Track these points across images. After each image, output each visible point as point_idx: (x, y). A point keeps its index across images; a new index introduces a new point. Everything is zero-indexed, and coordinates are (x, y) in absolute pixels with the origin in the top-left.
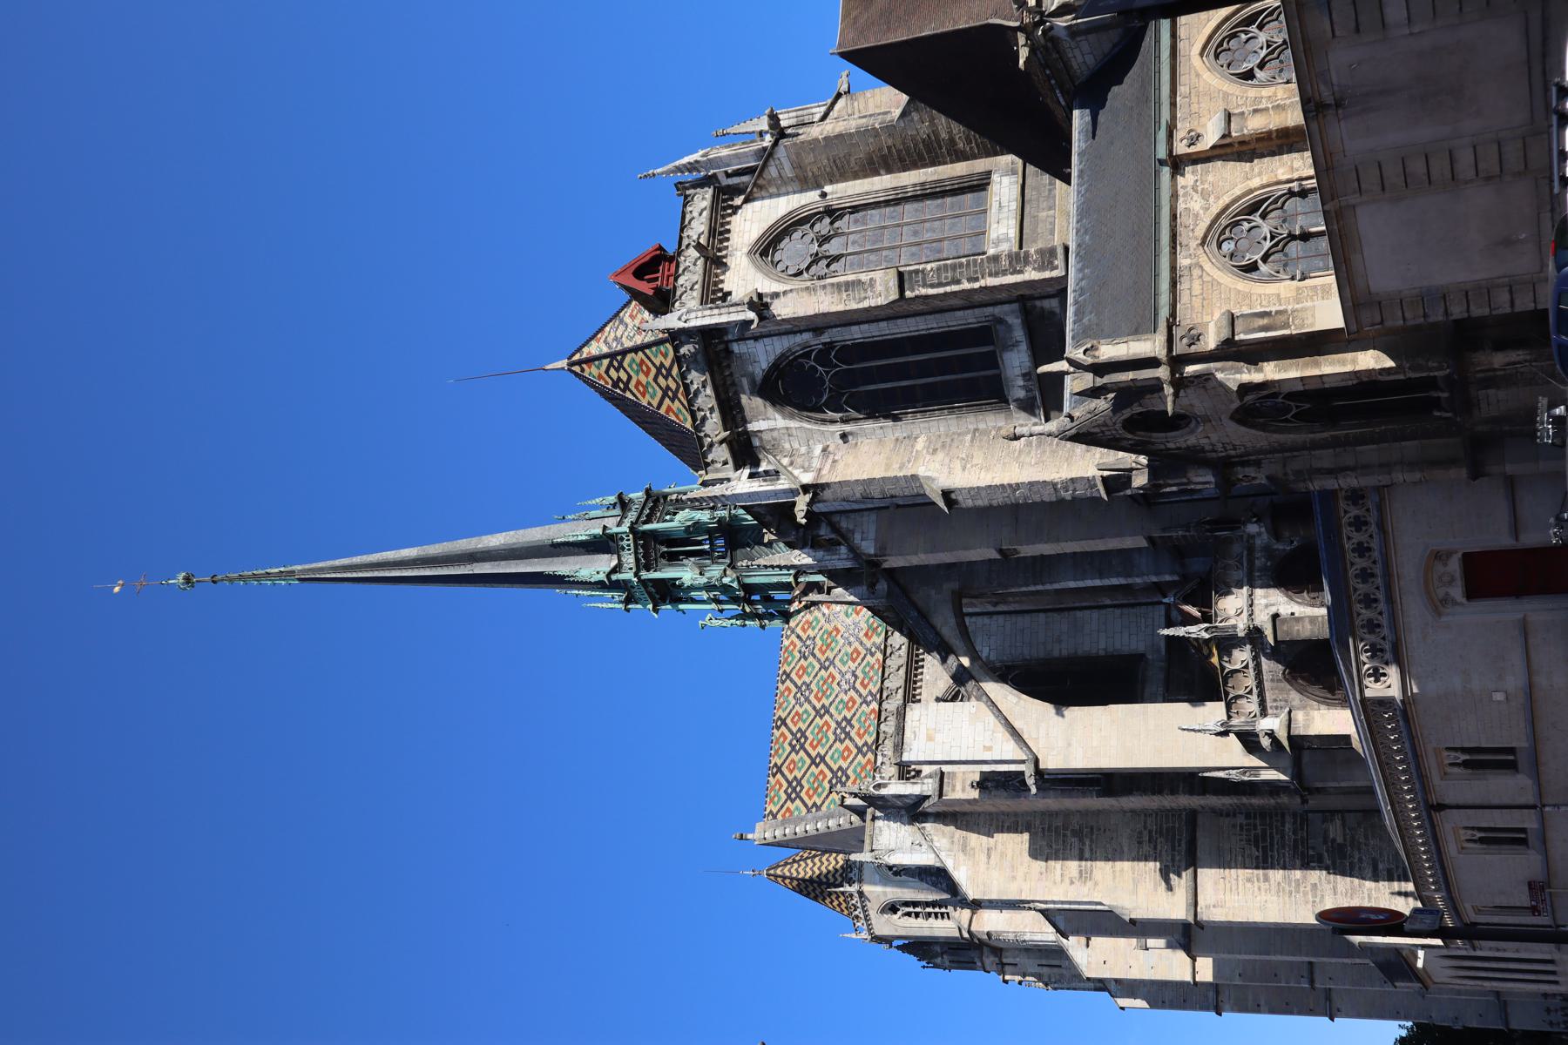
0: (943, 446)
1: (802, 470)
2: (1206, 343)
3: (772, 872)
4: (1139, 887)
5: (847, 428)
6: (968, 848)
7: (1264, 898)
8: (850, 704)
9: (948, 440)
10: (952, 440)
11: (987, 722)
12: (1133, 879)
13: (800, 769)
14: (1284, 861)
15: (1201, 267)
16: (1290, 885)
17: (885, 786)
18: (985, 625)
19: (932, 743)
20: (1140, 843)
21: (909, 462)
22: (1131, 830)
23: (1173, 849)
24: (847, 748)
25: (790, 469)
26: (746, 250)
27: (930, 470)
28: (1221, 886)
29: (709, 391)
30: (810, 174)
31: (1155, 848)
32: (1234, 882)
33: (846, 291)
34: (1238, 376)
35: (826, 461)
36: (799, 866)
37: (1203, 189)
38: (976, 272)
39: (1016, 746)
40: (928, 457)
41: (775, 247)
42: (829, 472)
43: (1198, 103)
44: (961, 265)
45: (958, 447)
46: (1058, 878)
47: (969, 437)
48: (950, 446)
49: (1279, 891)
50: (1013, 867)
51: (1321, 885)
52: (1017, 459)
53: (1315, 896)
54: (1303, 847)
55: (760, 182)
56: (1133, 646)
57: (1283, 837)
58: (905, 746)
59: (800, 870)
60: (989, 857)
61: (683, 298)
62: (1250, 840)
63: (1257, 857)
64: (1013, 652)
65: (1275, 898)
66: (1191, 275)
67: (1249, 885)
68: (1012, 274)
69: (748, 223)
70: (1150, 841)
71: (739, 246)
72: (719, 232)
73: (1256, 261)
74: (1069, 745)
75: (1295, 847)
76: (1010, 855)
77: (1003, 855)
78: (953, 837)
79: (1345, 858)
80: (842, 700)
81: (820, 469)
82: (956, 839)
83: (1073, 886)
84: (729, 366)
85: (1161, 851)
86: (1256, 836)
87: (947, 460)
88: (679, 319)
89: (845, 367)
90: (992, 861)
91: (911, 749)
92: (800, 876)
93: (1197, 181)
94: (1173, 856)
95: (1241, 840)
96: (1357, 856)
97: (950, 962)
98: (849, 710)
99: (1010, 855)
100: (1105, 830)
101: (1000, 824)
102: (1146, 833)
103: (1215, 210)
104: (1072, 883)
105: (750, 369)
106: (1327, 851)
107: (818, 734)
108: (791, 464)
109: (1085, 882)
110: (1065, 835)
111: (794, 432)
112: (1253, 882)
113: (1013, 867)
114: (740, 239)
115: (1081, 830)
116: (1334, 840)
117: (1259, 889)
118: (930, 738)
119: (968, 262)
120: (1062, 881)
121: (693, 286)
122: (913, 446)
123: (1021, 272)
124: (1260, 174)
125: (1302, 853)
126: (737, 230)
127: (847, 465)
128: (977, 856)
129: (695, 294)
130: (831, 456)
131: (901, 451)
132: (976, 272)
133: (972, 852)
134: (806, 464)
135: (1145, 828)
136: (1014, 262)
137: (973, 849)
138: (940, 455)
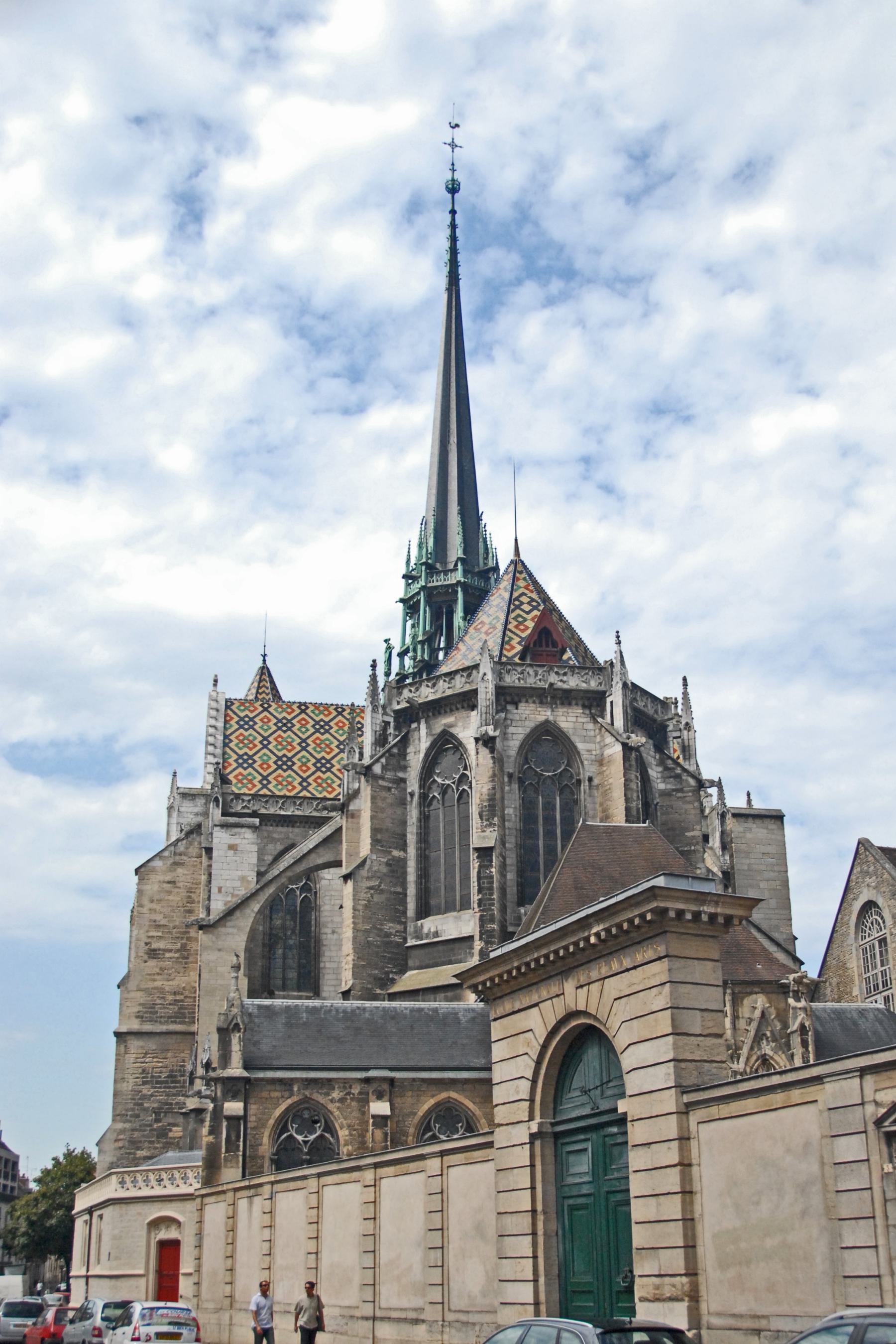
0: (393, 871)
1: (384, 764)
2: (230, 1101)
4: (142, 993)
5: (416, 798)
6: (176, 867)
7: (131, 1081)
8: (304, 768)
9: (399, 874)
10: (398, 878)
12: (148, 988)
13: (261, 727)
14: (157, 1096)
15: (290, 1097)
16: (140, 1099)
17: (218, 806)
20: (175, 993)
21: (382, 846)
22: (184, 987)
23: (169, 1017)
24: (269, 766)
25: (387, 755)
26: (551, 718)
27: (372, 862)
28: (140, 1051)
29: (449, 692)
30: (605, 769)
31: (170, 1004)
32: (143, 1060)
33: (489, 805)
34: (208, 1119)
35: (390, 782)
37: (347, 1099)
38: (485, 905)
40: (385, 860)
41: (553, 741)
42: (380, 786)
43: (412, 1096)
44: (492, 894)
45: (391, 882)
46: (151, 934)
47: (399, 890)
48: (393, 876)
49: (135, 1091)
51: (139, 1121)
52: (374, 927)
53: (131, 1116)
54: (167, 1109)
55: (603, 730)
56: (325, 988)
57: (174, 1095)
60: (169, 882)
61: (514, 672)
62: (173, 1072)
63: (160, 1077)
65: (130, 1089)
66: (285, 1091)
67: (140, 1070)
68: (480, 932)
69: (574, 719)
70: (175, 1000)
71: (555, 713)
72: (566, 698)
73: (289, 1131)
74: (220, 950)
75: (167, 1104)
76: (171, 898)
79: (158, 1137)
80: (309, 761)
81: (382, 778)
83: (143, 944)
84: (463, 707)
85: (168, 1008)
86: (175, 1076)
87: (378, 874)
88: (485, 674)
89: (456, 797)
90: (165, 885)
93: (353, 1094)
94: (164, 1017)
95: (173, 1066)
96: (158, 1145)
98: (300, 767)
99: (171, 898)
100: (185, 968)
102: (182, 997)
103: (331, 1107)
104: (147, 944)
105: (460, 724)
106: (163, 1125)
107: (287, 742)
108: (392, 755)
109: (147, 954)
110: (182, 938)
111: (416, 757)
112: (141, 1073)
113: (161, 900)
114: (561, 713)
115: (186, 950)
116: (171, 1130)
117: (137, 1078)
118: (232, 847)
119: (493, 899)
120: (149, 937)
121: (523, 679)
122: (396, 848)
123: (481, 939)
124: (351, 1135)
125: (162, 1108)
126: (570, 711)
127: (384, 799)
128: (170, 873)
129: (517, 681)
130: (395, 786)
131: (394, 840)
132: (485, 905)
134: (390, 767)
135: (186, 997)
136: (489, 934)
137: (175, 870)
138: (384, 870)
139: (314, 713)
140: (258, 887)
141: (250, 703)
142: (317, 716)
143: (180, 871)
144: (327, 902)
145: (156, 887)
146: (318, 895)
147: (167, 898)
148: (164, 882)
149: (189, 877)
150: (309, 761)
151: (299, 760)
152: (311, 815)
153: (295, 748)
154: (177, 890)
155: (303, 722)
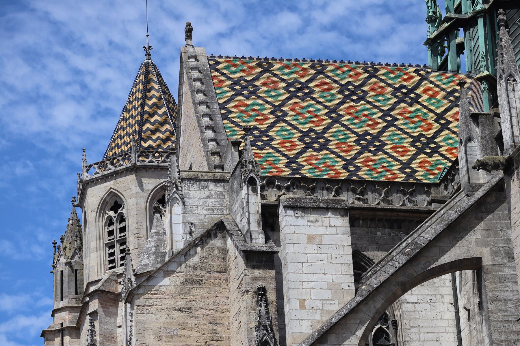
3: (151, 68)
6: (190, 286)
11: (332, 302)
18: (443, 297)
19: (306, 242)
24: (294, 145)
36: (159, 99)
39: (307, 336)
50: (172, 337)
58: (299, 213)
59: (154, 100)
64: (413, 330)
77: (184, 326)
78: (201, 269)
82: (199, 272)
90: (177, 314)
91: (297, 217)
92: (147, 100)
97: (62, 272)
98: (338, 145)
101: (219, 321)
107: (309, 112)
118: (311, 239)
128: (181, 296)
133: (185, 290)
139: (336, 74)
140: (359, 299)
141: (241, 62)
142: (341, 78)
143: (196, 291)
144: (413, 336)
145: (163, 317)
146: (399, 327)
147: (181, 332)
148: (174, 309)
149: (210, 301)
150: (349, 137)
151: (333, 136)
152: (379, 206)
153: (323, 120)
154: (195, 321)
155: (325, 87)
